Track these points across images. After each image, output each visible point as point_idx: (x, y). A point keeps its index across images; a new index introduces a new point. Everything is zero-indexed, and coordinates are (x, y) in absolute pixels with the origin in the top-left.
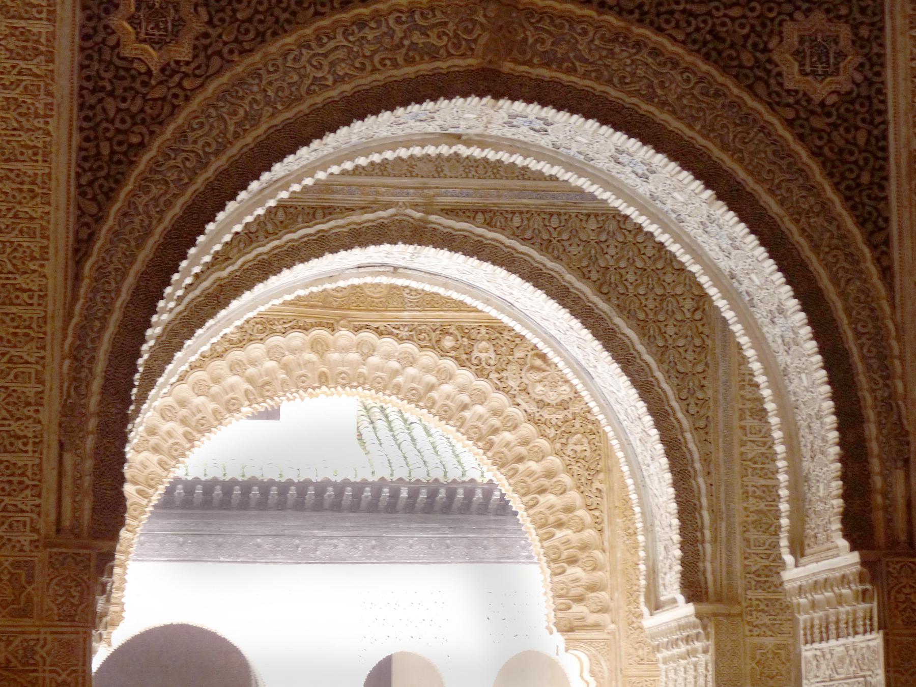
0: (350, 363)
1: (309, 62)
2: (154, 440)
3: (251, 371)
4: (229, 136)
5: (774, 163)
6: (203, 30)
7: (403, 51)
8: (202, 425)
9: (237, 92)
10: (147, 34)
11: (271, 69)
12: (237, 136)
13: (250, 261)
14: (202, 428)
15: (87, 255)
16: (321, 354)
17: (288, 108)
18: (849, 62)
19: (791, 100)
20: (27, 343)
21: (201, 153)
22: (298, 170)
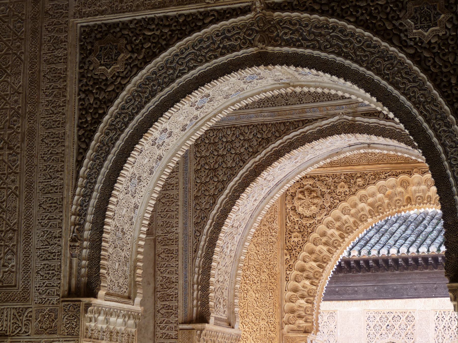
0: (423, 191)
1: (177, 62)
2: (324, 239)
3: (370, 200)
5: (406, 78)
6: (129, 56)
8: (348, 229)
10: (104, 61)
11: (161, 69)
12: (146, 103)
13: (269, 152)
14: (348, 231)
15: (81, 167)
16: (406, 188)
17: (167, 86)
18: (444, 18)
19: (412, 43)
20: (55, 210)
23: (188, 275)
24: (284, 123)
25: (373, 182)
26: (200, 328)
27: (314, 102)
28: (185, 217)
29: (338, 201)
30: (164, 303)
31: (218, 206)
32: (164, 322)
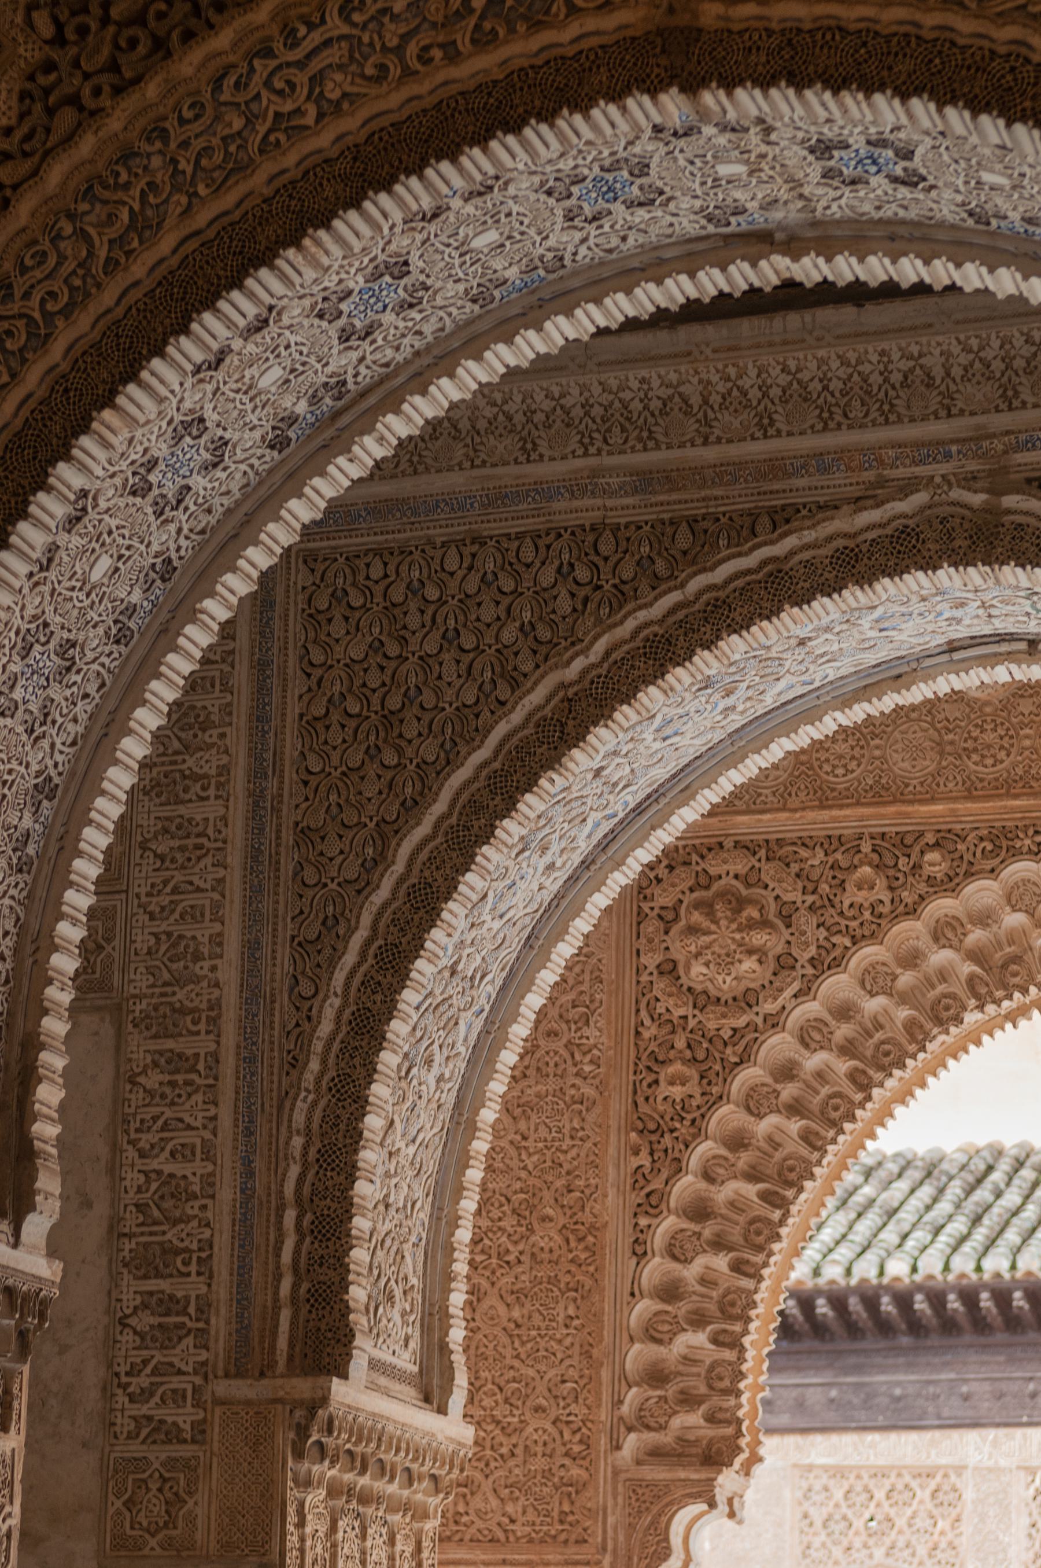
1: (268, 84)
2: (788, 1091)
3: (976, 936)
4: (97, 268)
7: (472, 21)
8: (887, 1054)
9: (118, 174)
12: (112, 266)
13: (625, 642)
17: (218, 190)
21: (37, 315)
22: (407, 362)
23: (258, 1164)
24: (692, 522)
25: (989, 864)
26: (307, 1395)
27: (825, 428)
28: (252, 918)
29: (848, 944)
30: (152, 1285)
31: (399, 867)
32: (148, 1370)
